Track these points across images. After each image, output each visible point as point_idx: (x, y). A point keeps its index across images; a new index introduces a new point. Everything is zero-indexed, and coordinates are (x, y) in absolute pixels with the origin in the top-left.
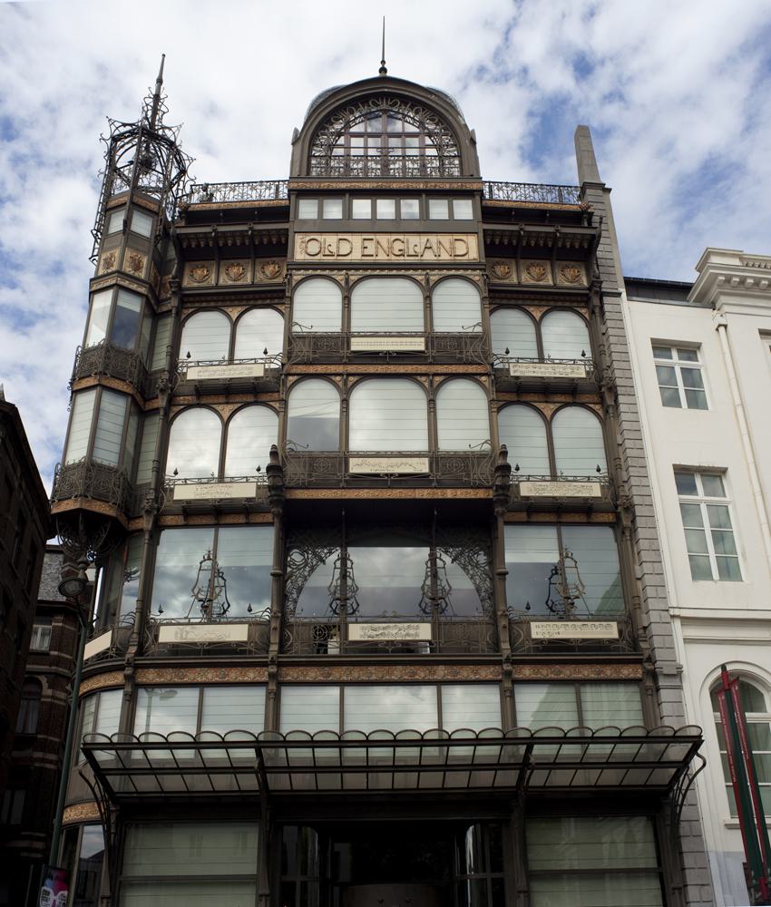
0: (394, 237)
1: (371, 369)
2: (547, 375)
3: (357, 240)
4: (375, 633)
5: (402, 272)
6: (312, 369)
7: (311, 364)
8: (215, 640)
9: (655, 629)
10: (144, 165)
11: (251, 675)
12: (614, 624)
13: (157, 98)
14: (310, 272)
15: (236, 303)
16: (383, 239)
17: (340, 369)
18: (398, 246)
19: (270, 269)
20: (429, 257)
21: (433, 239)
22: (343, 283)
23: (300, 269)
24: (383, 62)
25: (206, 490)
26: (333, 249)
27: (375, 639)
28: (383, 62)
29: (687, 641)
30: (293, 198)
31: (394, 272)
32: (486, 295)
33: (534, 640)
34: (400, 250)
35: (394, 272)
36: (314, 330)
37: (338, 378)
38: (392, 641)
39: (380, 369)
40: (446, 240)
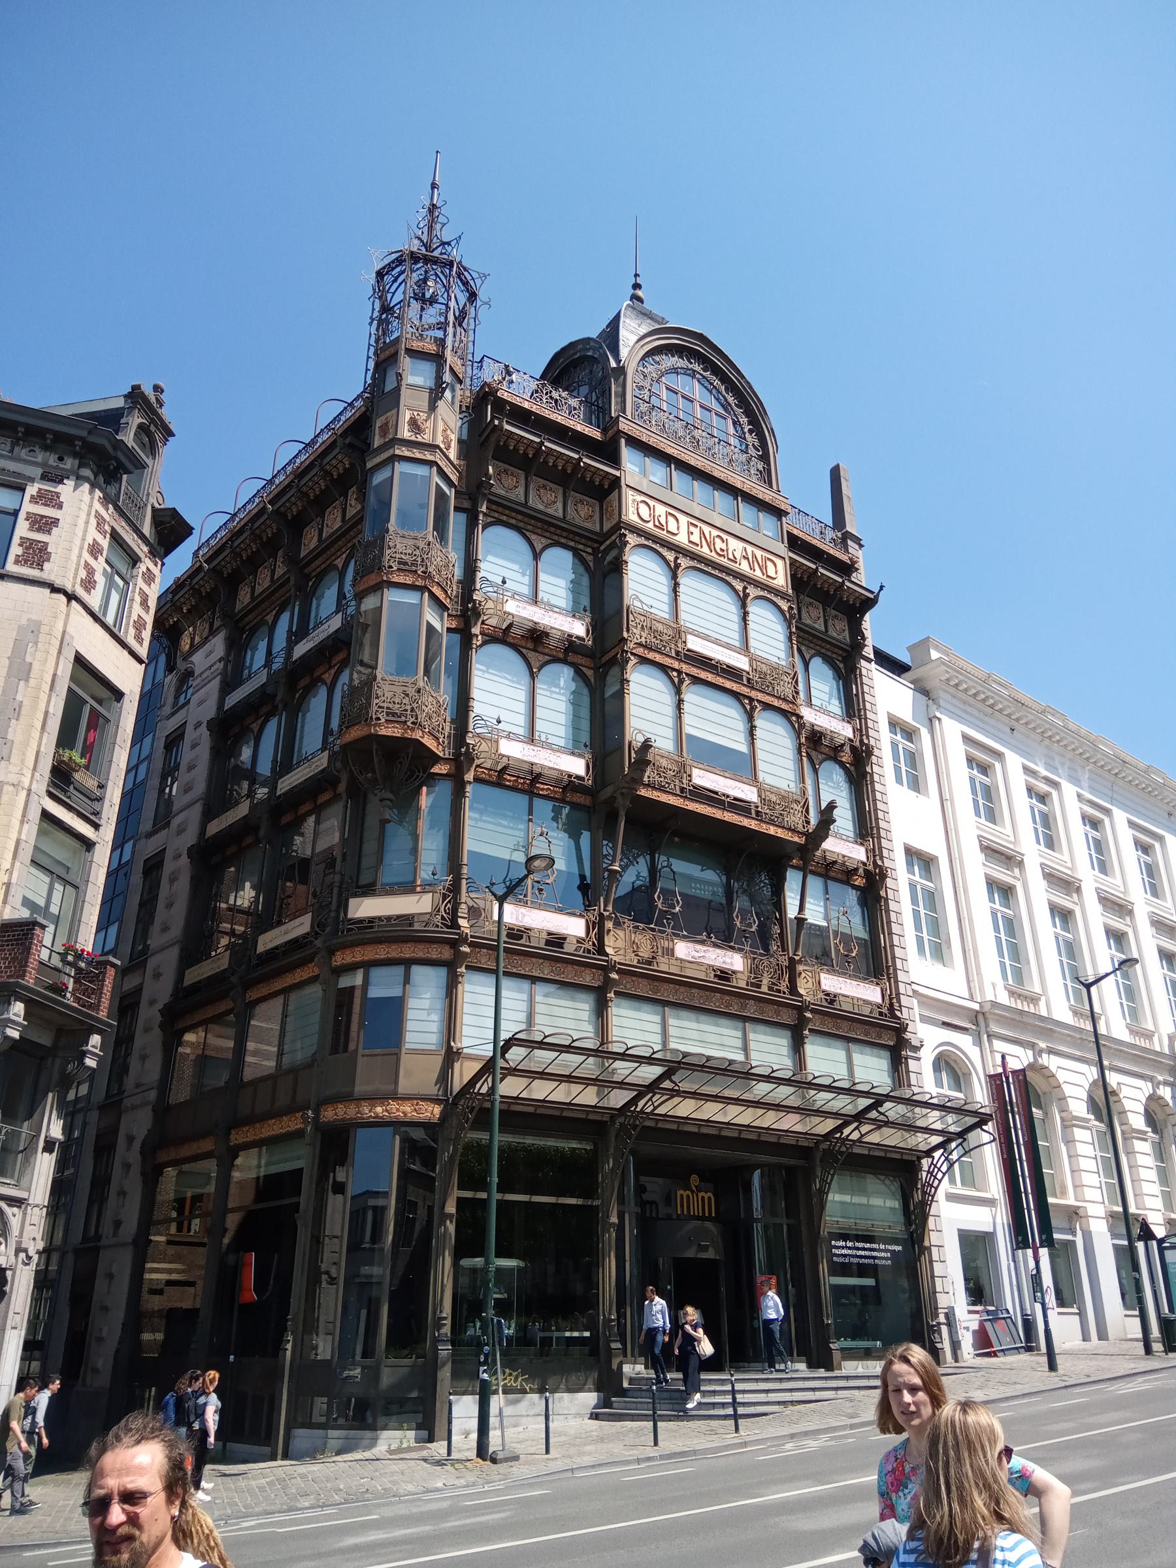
0: (715, 532)
1: (703, 675)
3: (683, 519)
5: (723, 576)
6: (651, 656)
7: (651, 649)
8: (553, 929)
9: (904, 1001)
11: (587, 978)
12: (878, 989)
15: (539, 531)
16: (706, 529)
17: (676, 665)
18: (719, 545)
19: (584, 511)
20: (744, 567)
21: (750, 549)
22: (672, 565)
23: (633, 532)
25: (533, 753)
26: (663, 522)
29: (924, 1019)
30: (623, 441)
31: (716, 573)
32: (794, 630)
34: (722, 550)
35: (716, 573)
37: (675, 674)
39: (710, 677)
40: (759, 553)
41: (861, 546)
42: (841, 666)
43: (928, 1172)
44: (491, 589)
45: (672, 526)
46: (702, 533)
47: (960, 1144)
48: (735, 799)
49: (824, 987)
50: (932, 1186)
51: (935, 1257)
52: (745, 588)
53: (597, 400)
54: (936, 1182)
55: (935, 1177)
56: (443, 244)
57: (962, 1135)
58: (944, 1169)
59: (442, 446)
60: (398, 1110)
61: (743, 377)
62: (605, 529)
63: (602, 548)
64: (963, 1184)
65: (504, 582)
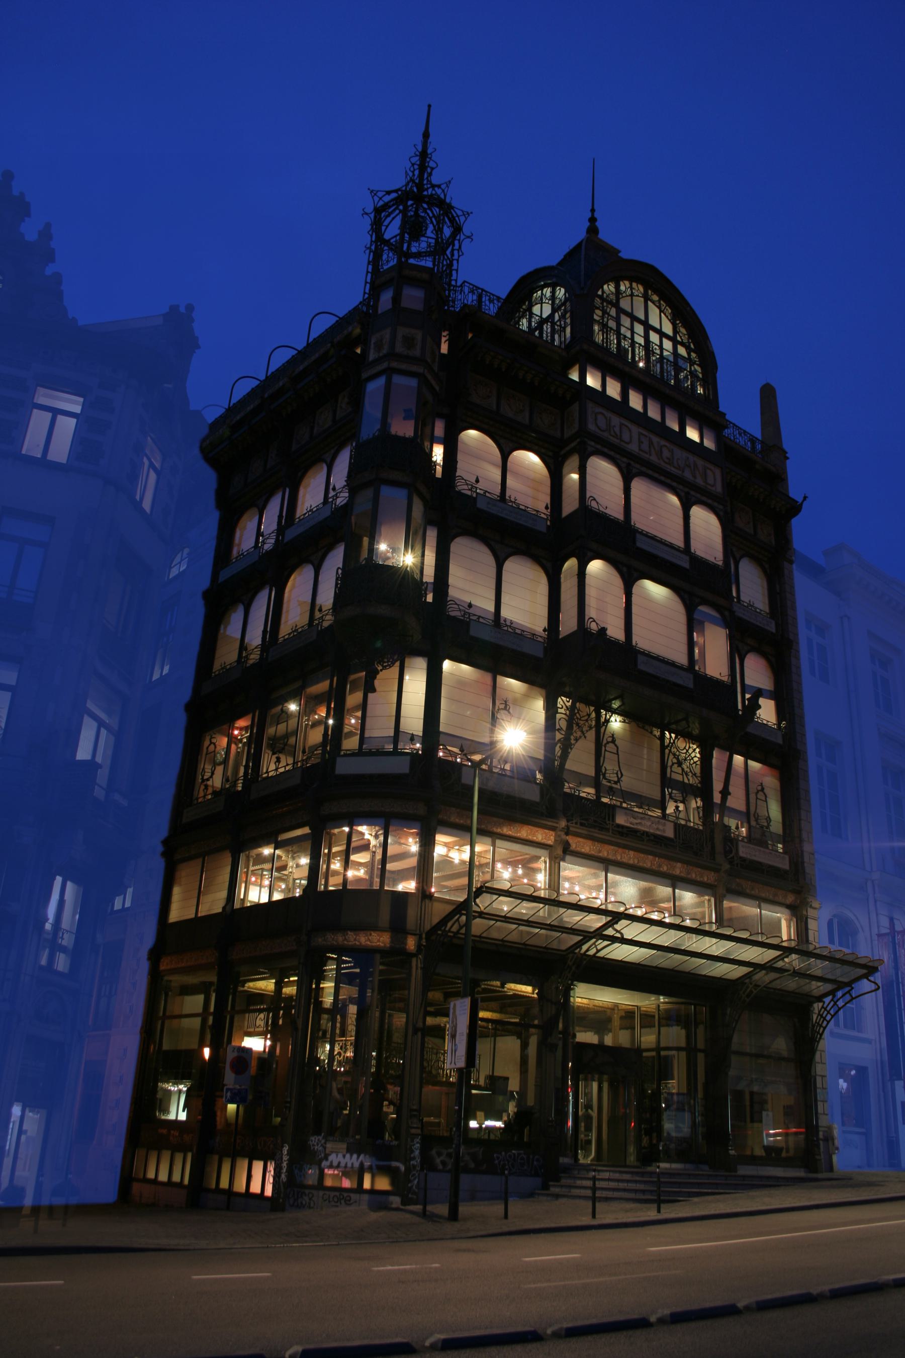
0: (663, 442)
2: (752, 621)
3: (635, 430)
4: (635, 821)
5: (668, 481)
10: (413, 228)
13: (424, 155)
14: (599, 447)
16: (655, 439)
20: (688, 475)
24: (593, 220)
27: (635, 827)
28: (593, 220)
33: (741, 857)
36: (606, 511)
38: (647, 833)
41: (788, 458)
42: (767, 566)
43: (819, 1014)
44: (466, 487)
45: (626, 437)
46: (651, 443)
47: (849, 992)
48: (675, 684)
49: (741, 854)
50: (821, 1026)
51: (819, 1085)
52: (687, 493)
53: (559, 320)
54: (825, 1023)
55: (825, 1019)
56: (433, 186)
57: (850, 984)
58: (832, 1012)
59: (429, 361)
60: (379, 941)
61: (688, 304)
62: (566, 436)
63: (562, 452)
64: (845, 1026)
65: (477, 481)
